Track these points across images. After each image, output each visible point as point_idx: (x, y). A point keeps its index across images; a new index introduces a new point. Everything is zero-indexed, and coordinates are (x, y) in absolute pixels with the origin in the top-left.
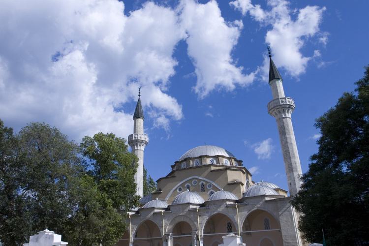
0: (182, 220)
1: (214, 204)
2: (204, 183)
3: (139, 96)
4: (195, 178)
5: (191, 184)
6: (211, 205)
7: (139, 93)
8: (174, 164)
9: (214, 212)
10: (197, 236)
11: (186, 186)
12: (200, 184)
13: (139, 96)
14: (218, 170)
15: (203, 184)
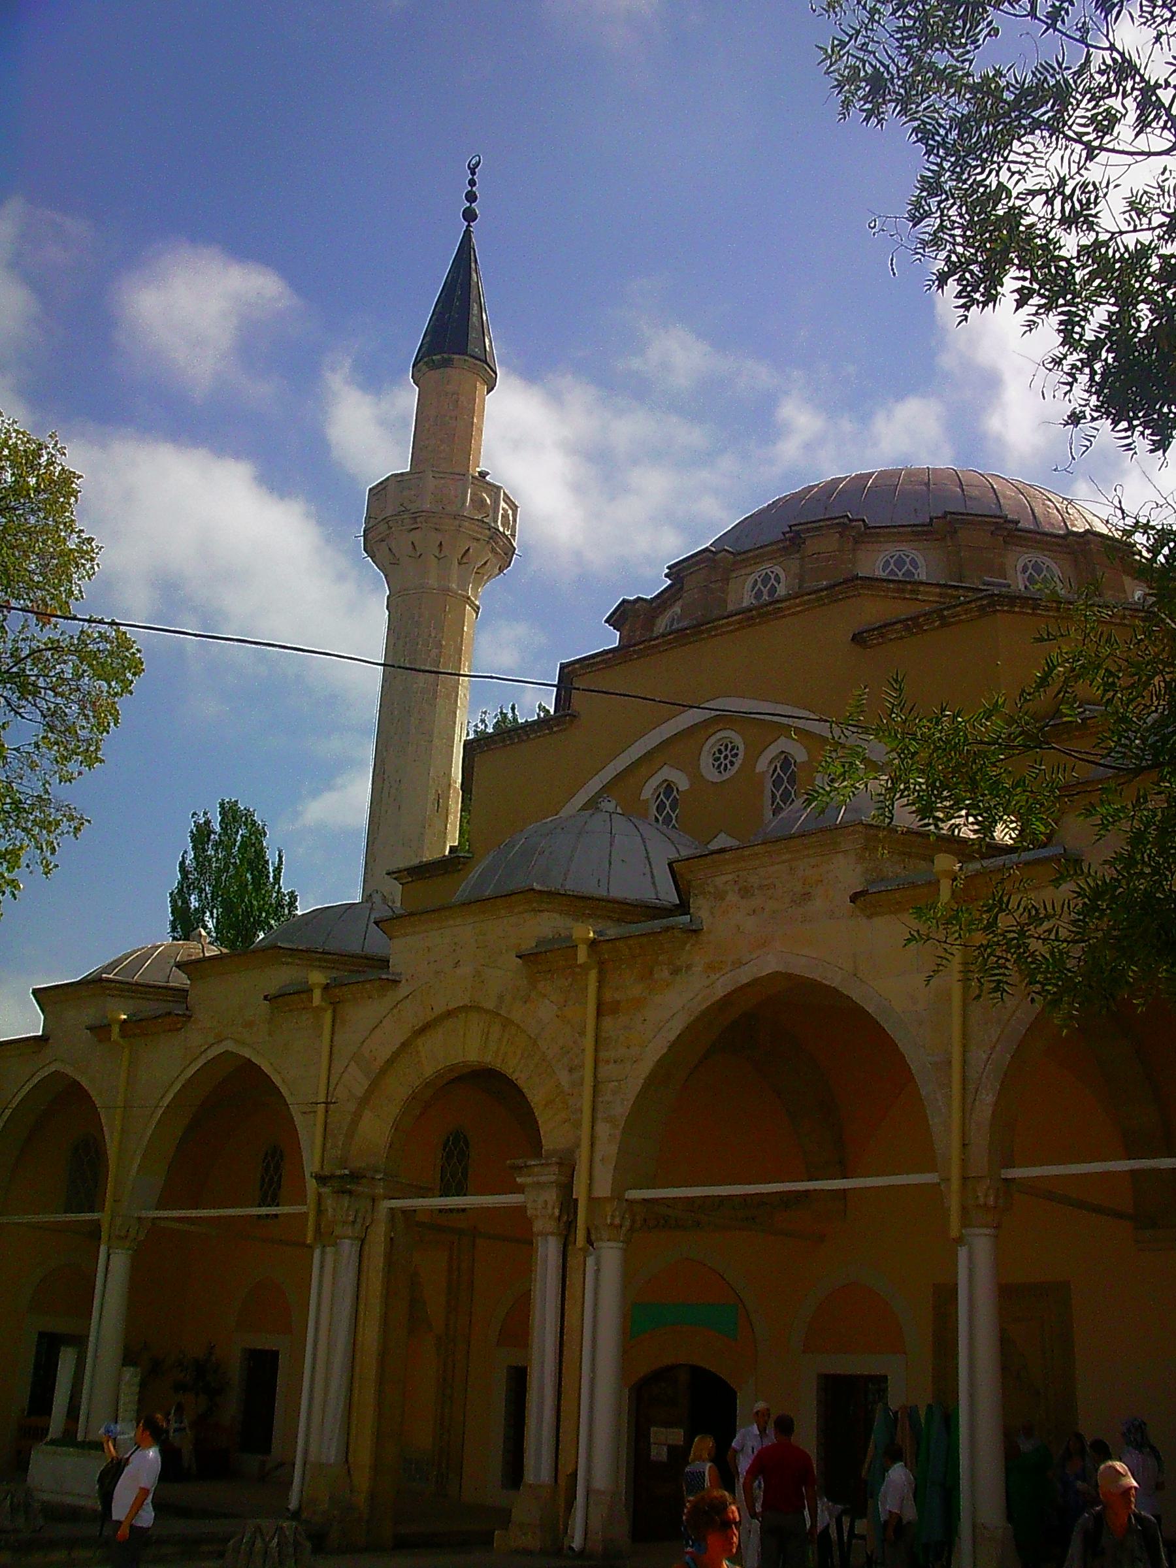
0: (469, 1046)
1: (745, 892)
2: (800, 754)
3: (470, 216)
4: (724, 719)
5: (695, 776)
6: (720, 896)
7: (471, 197)
8: (612, 639)
9: (739, 964)
10: (568, 1204)
11: (647, 793)
12: (762, 765)
13: (470, 216)
14: (912, 625)
15: (786, 761)
